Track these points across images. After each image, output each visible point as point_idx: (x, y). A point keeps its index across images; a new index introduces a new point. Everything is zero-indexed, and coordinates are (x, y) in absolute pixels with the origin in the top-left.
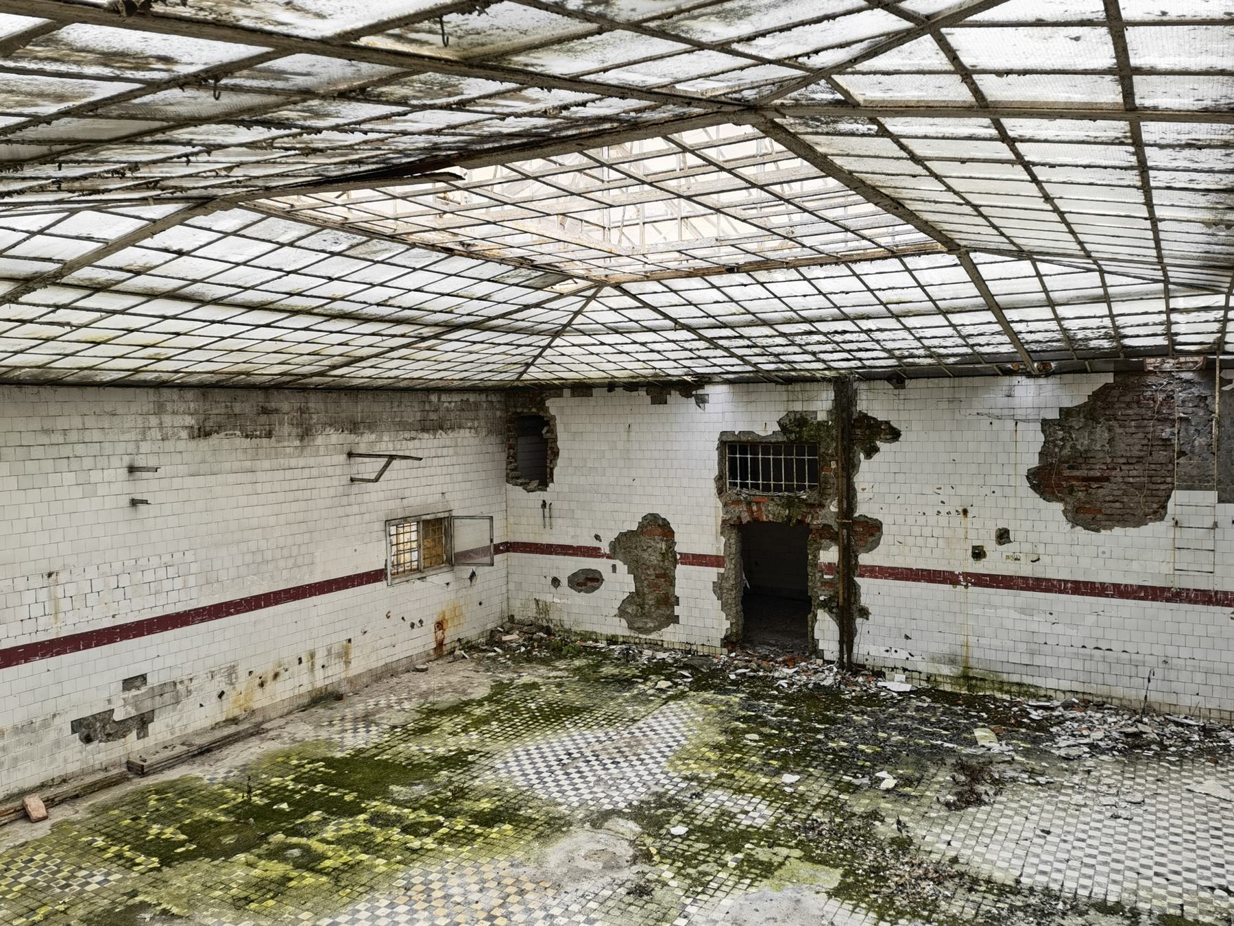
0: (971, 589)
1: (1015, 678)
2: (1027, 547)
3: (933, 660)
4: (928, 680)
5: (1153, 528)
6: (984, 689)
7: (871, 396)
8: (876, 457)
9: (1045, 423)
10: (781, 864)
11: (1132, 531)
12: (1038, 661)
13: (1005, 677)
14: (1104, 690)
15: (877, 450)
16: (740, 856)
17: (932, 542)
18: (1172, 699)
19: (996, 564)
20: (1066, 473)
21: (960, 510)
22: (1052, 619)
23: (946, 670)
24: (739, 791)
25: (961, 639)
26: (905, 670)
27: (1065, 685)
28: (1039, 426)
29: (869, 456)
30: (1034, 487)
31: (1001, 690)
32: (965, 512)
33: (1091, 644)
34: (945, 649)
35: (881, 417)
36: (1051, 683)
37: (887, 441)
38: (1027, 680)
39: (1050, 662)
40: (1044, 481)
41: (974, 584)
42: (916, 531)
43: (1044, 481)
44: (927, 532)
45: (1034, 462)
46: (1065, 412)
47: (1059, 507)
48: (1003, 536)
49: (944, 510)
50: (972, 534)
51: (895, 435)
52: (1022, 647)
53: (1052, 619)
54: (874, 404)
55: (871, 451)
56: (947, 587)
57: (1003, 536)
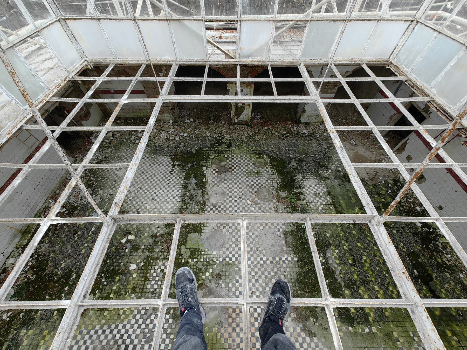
3: (10, 244)
4: (17, 248)
10: (190, 248)
12: (32, 205)
14: (50, 191)
16: (190, 260)
18: (61, 176)
22: (19, 193)
23: (17, 240)
24: (146, 279)
26: (8, 258)
27: (43, 201)
33: (35, 187)
36: (40, 205)
39: (34, 201)
53: (19, 193)
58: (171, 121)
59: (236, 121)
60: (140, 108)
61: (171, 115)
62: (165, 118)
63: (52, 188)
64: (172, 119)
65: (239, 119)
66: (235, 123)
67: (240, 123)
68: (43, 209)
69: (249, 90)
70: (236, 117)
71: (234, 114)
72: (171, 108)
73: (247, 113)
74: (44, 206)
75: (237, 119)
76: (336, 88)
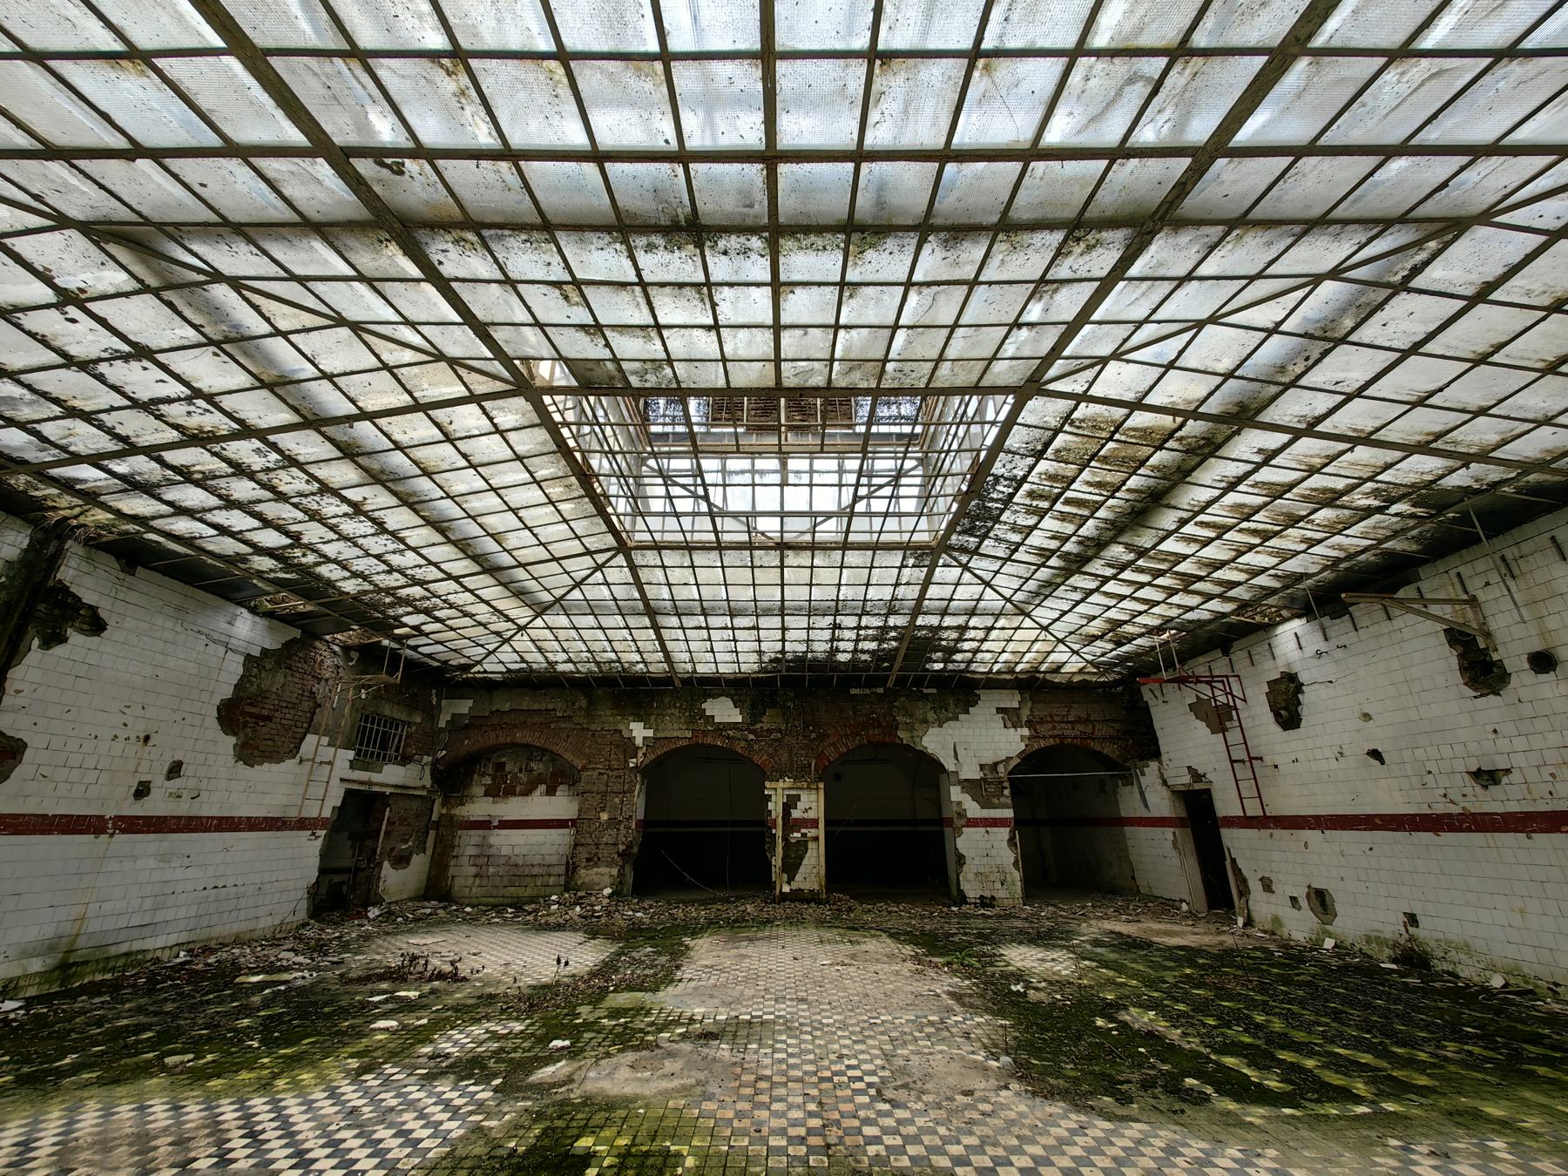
0: (119, 837)
1: (124, 948)
2: (192, 783)
5: (290, 764)
6: (82, 976)
7: (84, 567)
8: (59, 650)
9: (248, 657)
11: (275, 767)
13: (113, 951)
15: (63, 640)
17: (93, 775)
19: (155, 805)
20: (248, 709)
21: (142, 736)
22: (186, 862)
25: (76, 911)
28: (241, 659)
29: (46, 644)
30: (220, 719)
31: (104, 971)
32: (147, 738)
34: (49, 932)
35: (89, 598)
37: (82, 631)
38: (137, 946)
40: (231, 715)
41: (123, 831)
42: (75, 760)
43: (231, 715)
44: (90, 762)
45: (227, 692)
46: (264, 651)
47: (232, 740)
48: (175, 770)
49: (122, 734)
50: (144, 768)
51: (96, 625)
52: (148, 903)
54: (81, 576)
55: (54, 638)
56: (87, 838)
57: (175, 770)
58: (608, 891)
59: (786, 889)
60: (535, 871)
61: (615, 871)
62: (596, 879)
63: (216, 932)
64: (611, 886)
65: (794, 886)
66: (784, 897)
67: (798, 896)
68: (149, 956)
69: (813, 797)
70: (785, 876)
71: (779, 863)
72: (622, 847)
73: (814, 861)
74: (158, 954)
75: (789, 883)
76: (1007, 792)
